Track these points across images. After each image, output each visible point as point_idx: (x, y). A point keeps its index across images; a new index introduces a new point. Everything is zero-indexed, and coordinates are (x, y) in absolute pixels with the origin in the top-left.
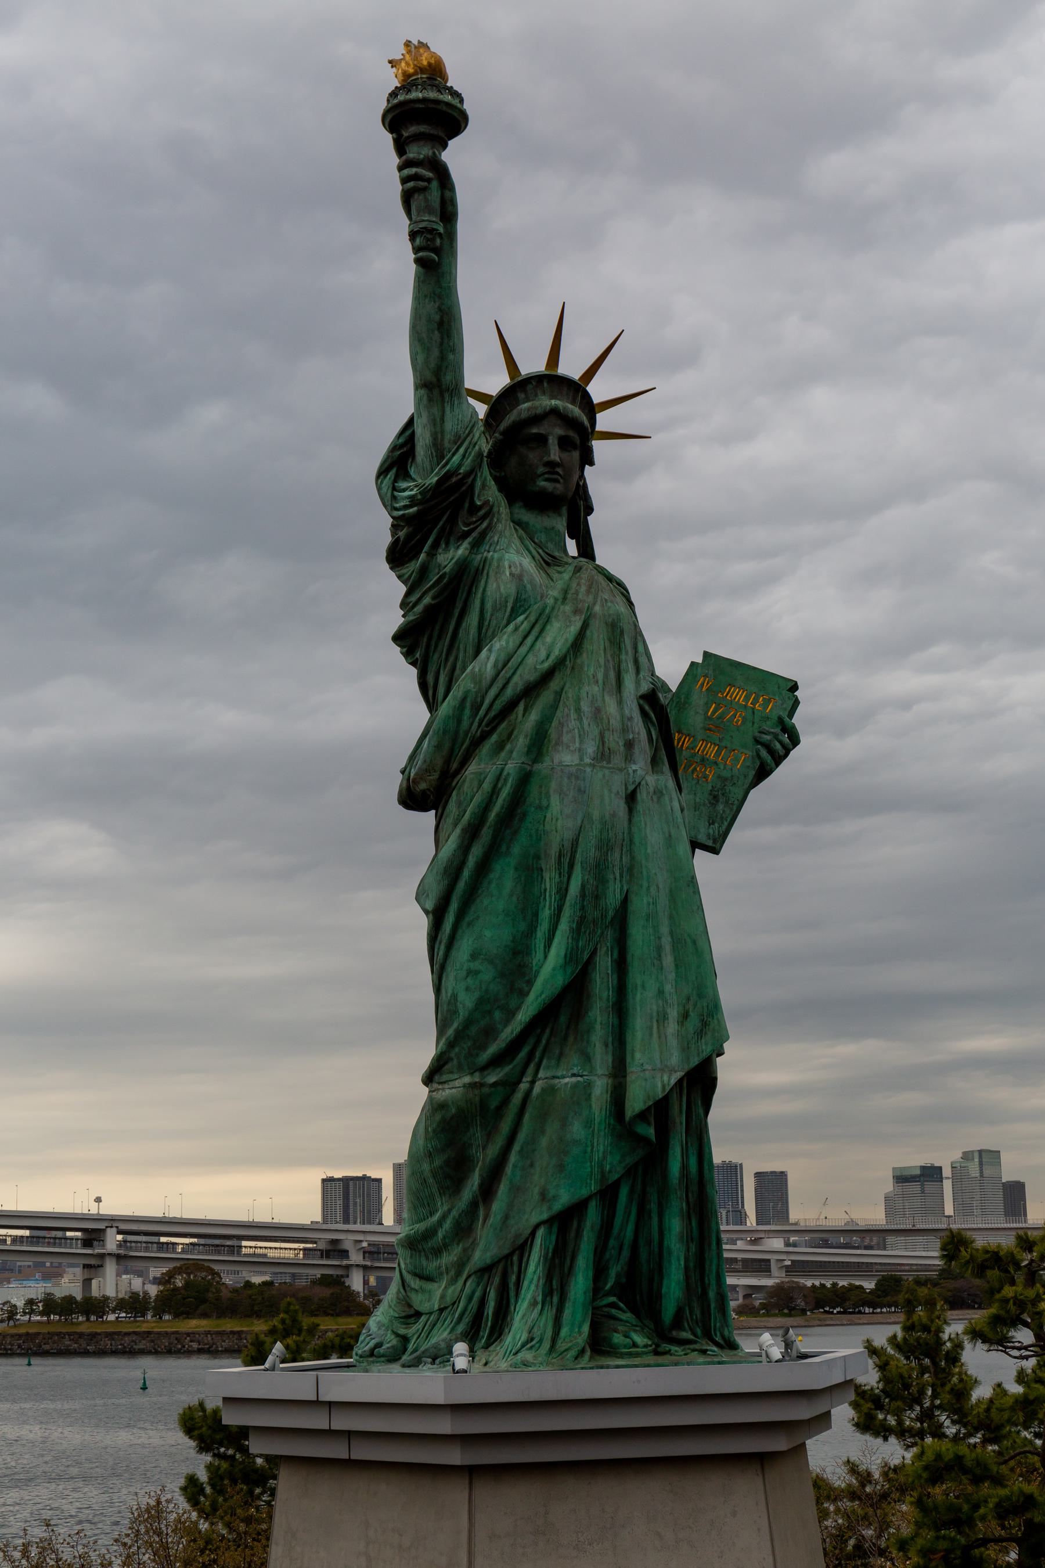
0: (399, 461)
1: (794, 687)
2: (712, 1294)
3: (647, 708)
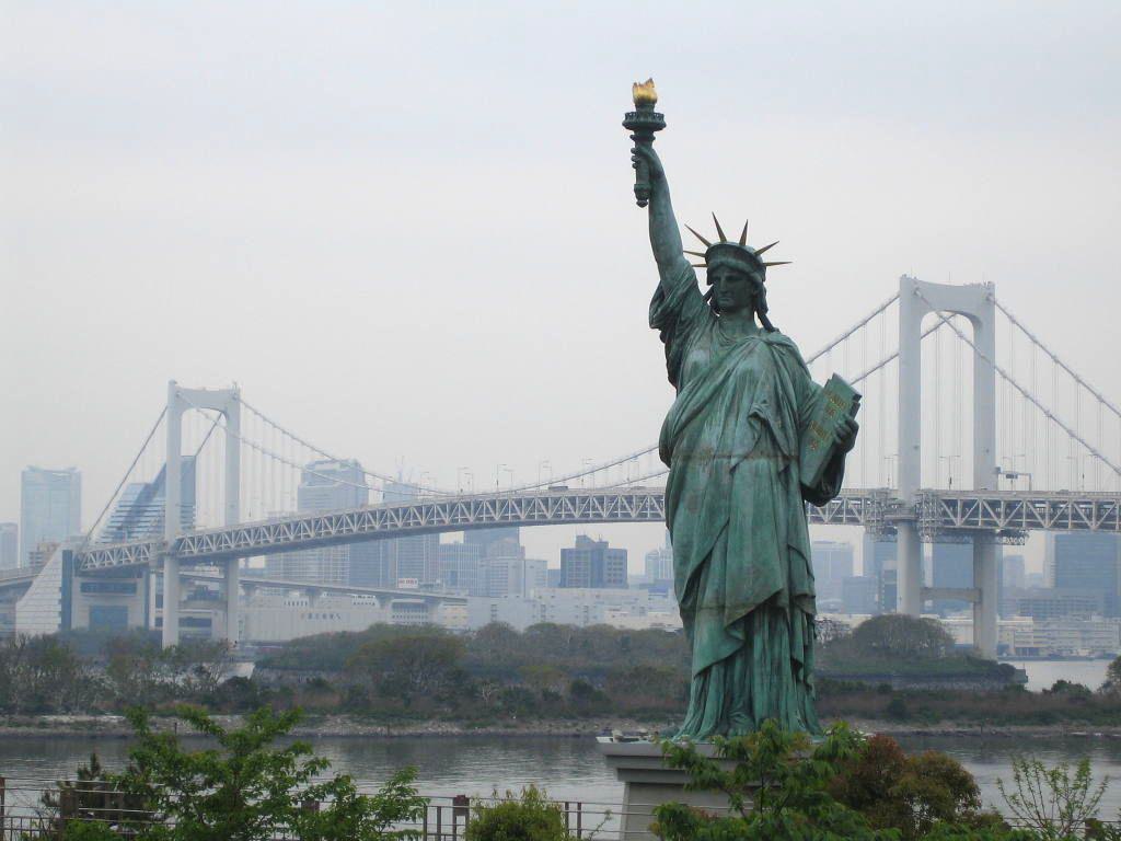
0: (660, 296)
1: (858, 397)
2: (783, 713)
3: (752, 422)
